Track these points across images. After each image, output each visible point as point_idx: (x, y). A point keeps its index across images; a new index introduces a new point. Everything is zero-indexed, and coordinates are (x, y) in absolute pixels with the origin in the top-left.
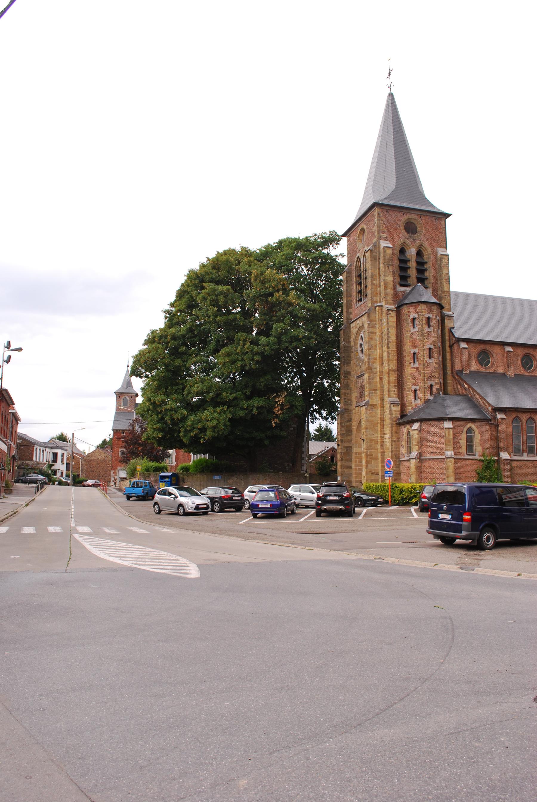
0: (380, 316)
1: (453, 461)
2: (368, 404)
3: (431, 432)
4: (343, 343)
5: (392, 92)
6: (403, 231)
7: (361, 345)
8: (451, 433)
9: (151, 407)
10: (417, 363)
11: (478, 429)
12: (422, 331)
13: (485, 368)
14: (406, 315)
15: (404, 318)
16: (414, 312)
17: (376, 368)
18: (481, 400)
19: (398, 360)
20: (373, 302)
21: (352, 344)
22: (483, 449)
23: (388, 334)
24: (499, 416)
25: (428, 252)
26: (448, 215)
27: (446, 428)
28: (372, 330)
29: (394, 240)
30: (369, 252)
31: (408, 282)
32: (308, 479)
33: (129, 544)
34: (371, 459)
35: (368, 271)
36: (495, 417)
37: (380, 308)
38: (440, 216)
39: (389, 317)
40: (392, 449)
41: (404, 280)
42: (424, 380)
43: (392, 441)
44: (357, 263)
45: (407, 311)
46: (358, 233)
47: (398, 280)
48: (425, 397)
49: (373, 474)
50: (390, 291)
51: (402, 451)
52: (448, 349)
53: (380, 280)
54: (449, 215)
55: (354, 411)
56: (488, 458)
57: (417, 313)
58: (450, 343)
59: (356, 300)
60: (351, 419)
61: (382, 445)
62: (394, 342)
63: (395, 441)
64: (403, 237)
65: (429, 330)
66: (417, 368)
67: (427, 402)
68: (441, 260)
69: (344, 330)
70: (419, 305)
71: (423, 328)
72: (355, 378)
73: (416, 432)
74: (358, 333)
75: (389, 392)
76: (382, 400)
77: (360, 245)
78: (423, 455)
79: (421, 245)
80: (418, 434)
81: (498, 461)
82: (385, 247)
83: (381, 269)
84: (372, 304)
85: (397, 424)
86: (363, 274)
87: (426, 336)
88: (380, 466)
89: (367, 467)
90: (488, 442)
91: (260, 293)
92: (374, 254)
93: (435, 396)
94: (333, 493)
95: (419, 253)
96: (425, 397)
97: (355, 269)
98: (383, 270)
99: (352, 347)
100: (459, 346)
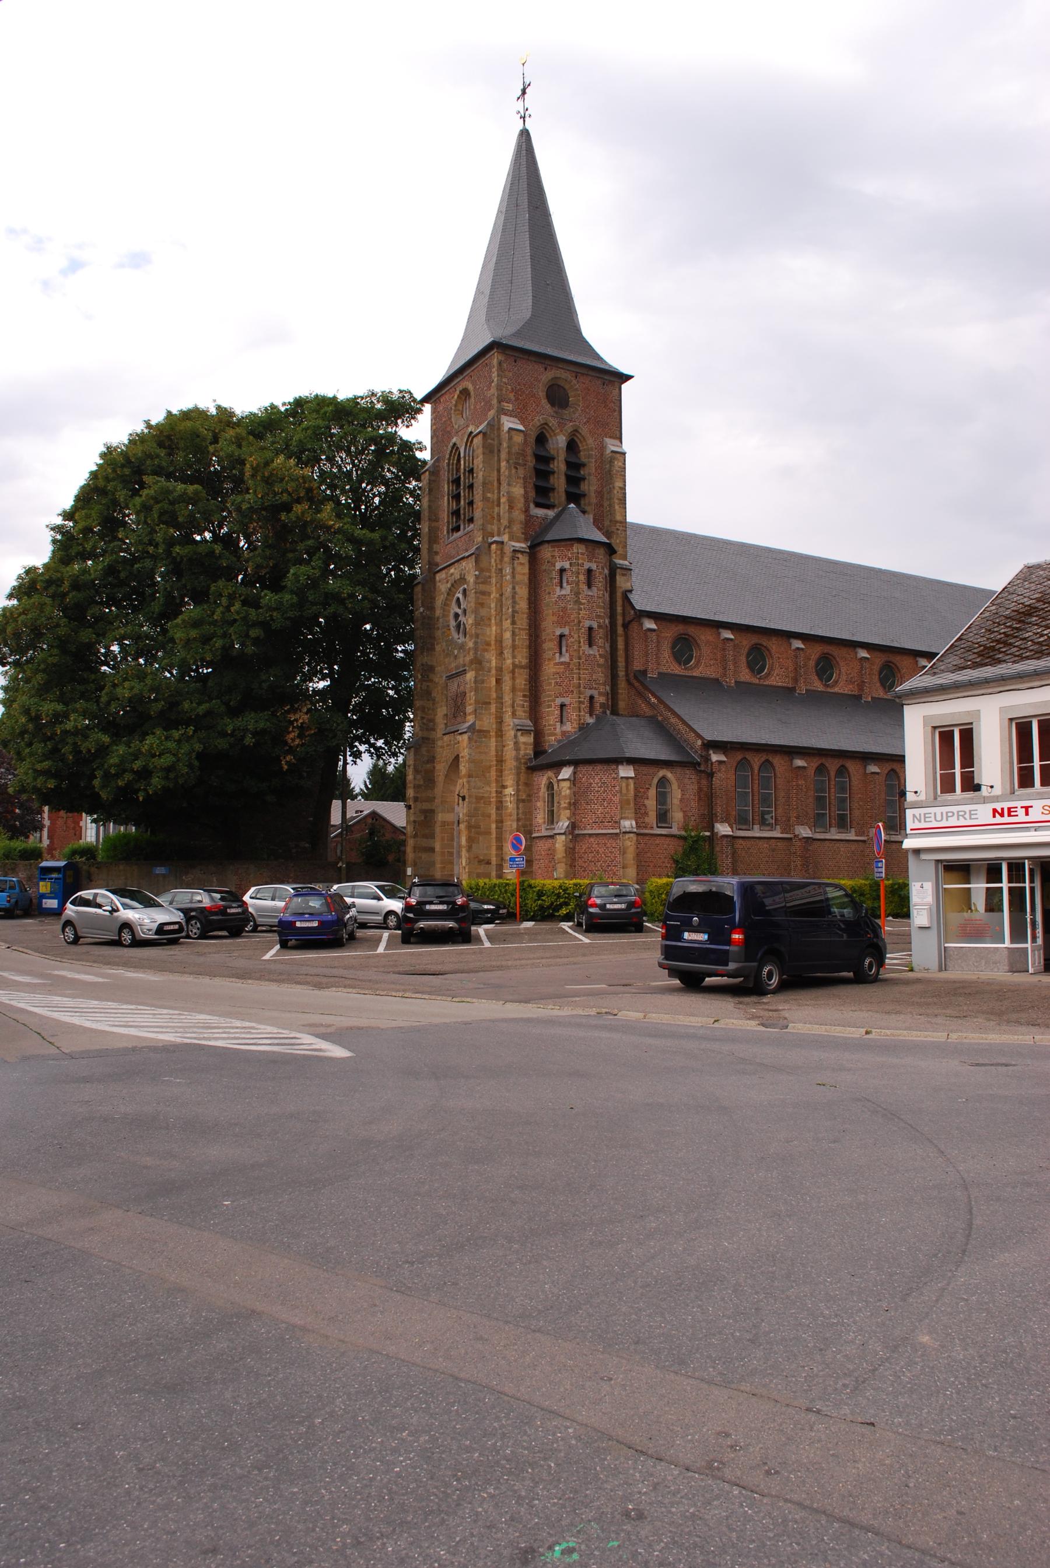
0: (498, 562)
1: (635, 838)
2: (474, 729)
4: (421, 610)
5: (527, 126)
6: (544, 402)
7: (457, 616)
8: (632, 786)
9: (31, 726)
10: (568, 655)
11: (678, 780)
12: (577, 594)
13: (686, 669)
14: (548, 562)
15: (544, 567)
16: (563, 558)
17: (490, 662)
18: (681, 726)
19: (530, 647)
20: (487, 534)
21: (438, 612)
22: (685, 816)
23: (513, 597)
24: (715, 758)
25: (588, 444)
26: (628, 378)
27: (622, 778)
28: (482, 587)
29: (526, 417)
30: (480, 437)
31: (549, 499)
32: (344, 872)
33: (109, 1003)
34: (478, 833)
35: (477, 473)
36: (707, 759)
37: (500, 546)
38: (612, 379)
39: (515, 565)
40: (518, 814)
41: (542, 494)
42: (580, 687)
43: (518, 800)
44: (450, 455)
45: (549, 554)
46: (456, 397)
47: (532, 494)
48: (580, 720)
49: (480, 862)
50: (519, 516)
51: (538, 820)
52: (620, 630)
53: (499, 493)
54: (629, 377)
55: (439, 743)
56: (693, 834)
57: (569, 559)
58: (624, 619)
59: (448, 527)
60: (434, 757)
61: (498, 809)
62: (523, 613)
63: (523, 801)
64: (544, 413)
65: (590, 593)
67: (583, 728)
68: (611, 461)
69: (423, 585)
70: (572, 545)
71: (579, 589)
72: (444, 678)
73: (567, 784)
74: (450, 592)
75: (513, 707)
76: (500, 721)
77: (458, 422)
78: (579, 828)
79: (576, 431)
80: (570, 788)
81: (712, 839)
82: (510, 429)
83: (502, 471)
84: (483, 538)
85: (528, 768)
86: (465, 479)
87: (584, 604)
88: (494, 848)
89: (469, 848)
90: (694, 804)
91: (263, 503)
92: (489, 441)
93: (598, 719)
94: (437, 897)
95: (572, 446)
96: (580, 720)
97: (446, 468)
98: (507, 473)
99: (438, 618)
100: (641, 625)
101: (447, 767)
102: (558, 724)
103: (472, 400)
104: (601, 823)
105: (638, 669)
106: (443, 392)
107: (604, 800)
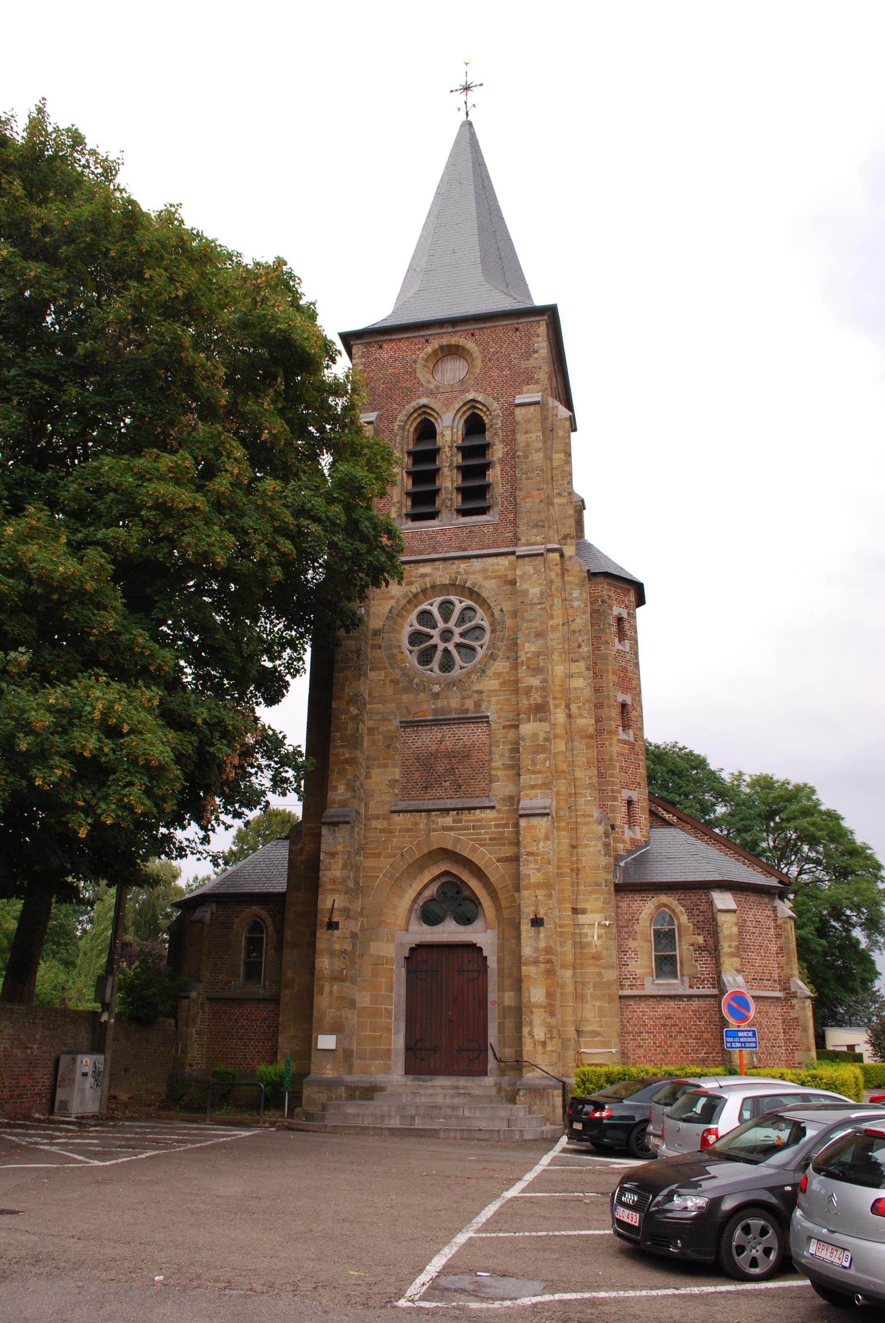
3: (749, 924)
5: (469, 118)
51: (630, 968)
101: (403, 866)
106: (393, 337)
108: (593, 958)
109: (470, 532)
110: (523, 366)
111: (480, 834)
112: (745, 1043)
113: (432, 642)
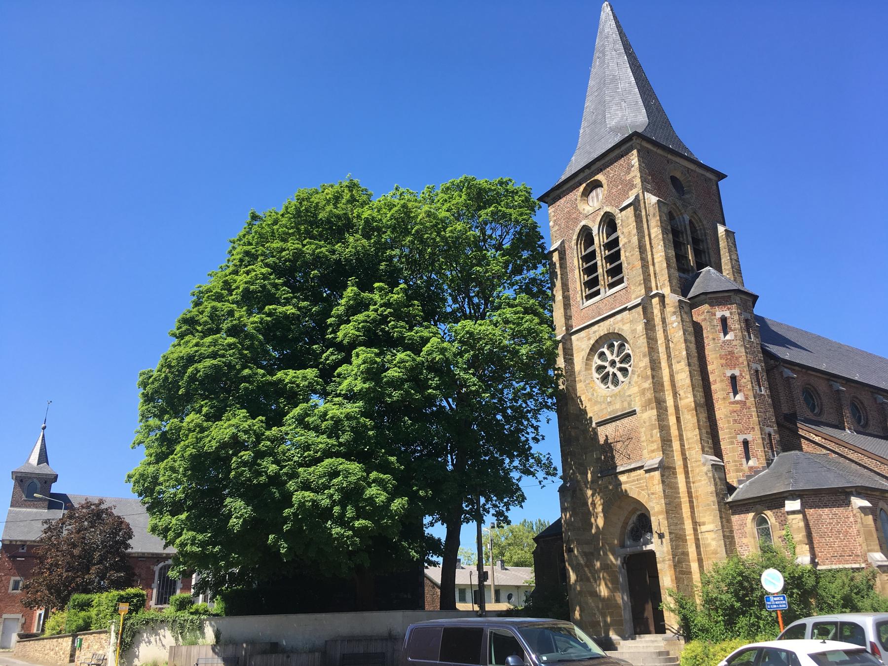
3: (824, 517)
6: (671, 186)
54: (724, 176)
66: (743, 403)
96: (766, 456)
102: (744, 460)
103: (605, 186)
104: (841, 557)
105: (785, 412)
107: (839, 532)
108: (713, 553)
109: (615, 297)
110: (628, 179)
111: (641, 483)
112: (778, 604)
113: (606, 370)
